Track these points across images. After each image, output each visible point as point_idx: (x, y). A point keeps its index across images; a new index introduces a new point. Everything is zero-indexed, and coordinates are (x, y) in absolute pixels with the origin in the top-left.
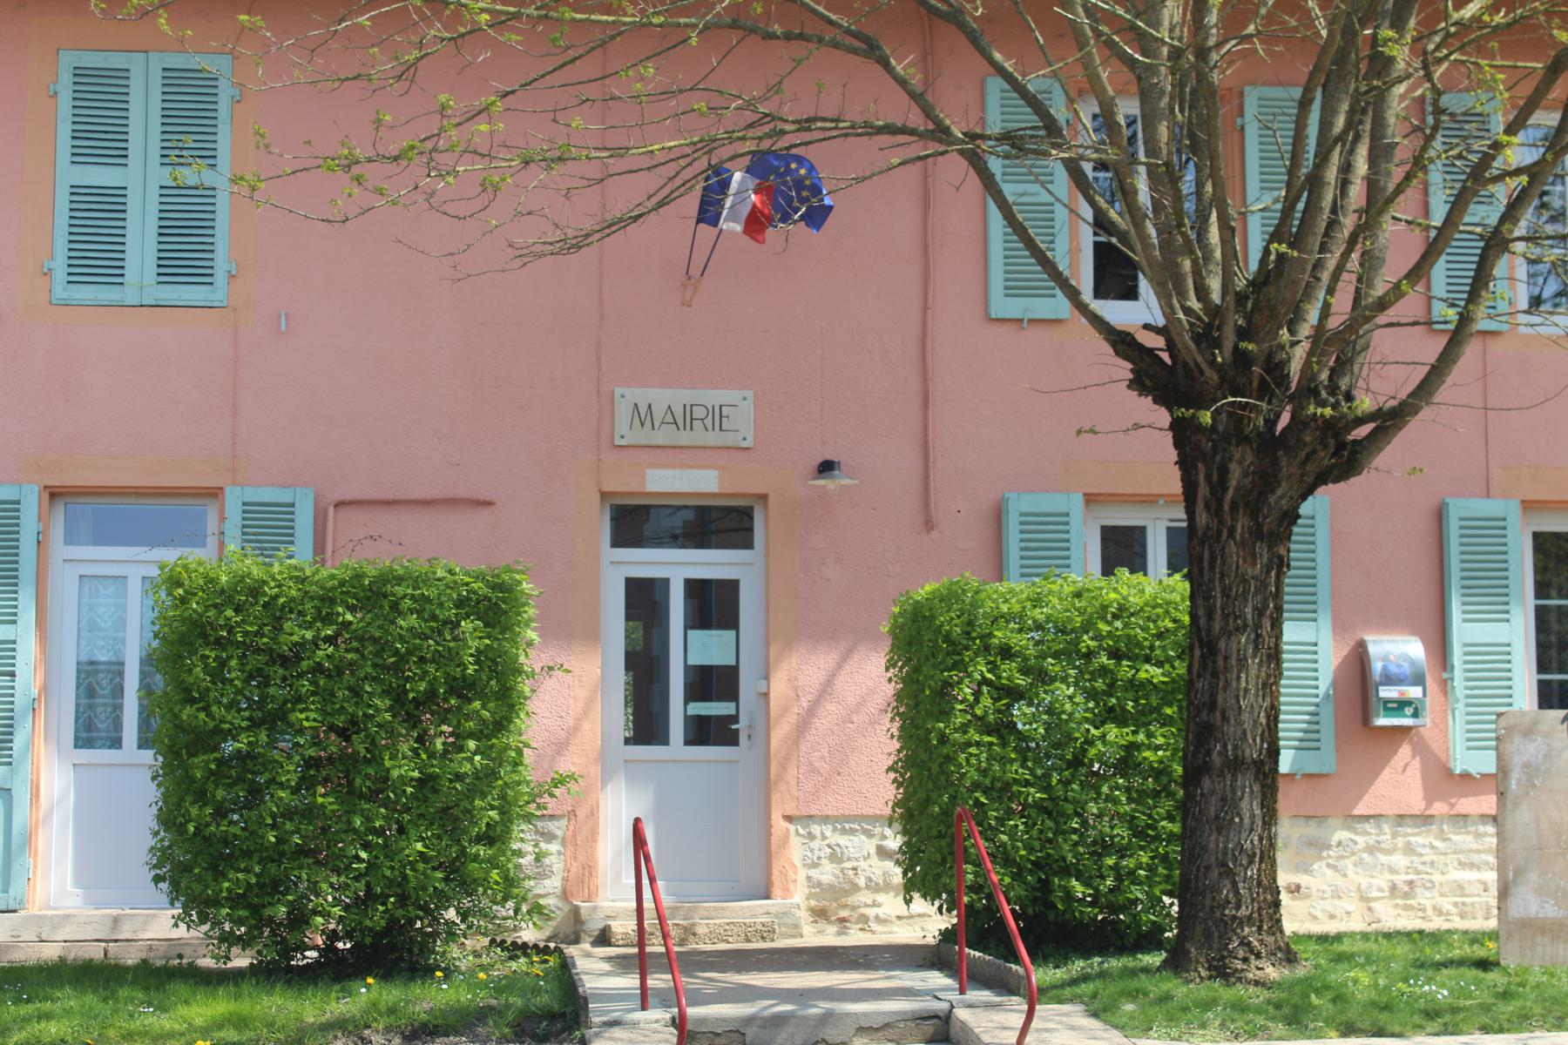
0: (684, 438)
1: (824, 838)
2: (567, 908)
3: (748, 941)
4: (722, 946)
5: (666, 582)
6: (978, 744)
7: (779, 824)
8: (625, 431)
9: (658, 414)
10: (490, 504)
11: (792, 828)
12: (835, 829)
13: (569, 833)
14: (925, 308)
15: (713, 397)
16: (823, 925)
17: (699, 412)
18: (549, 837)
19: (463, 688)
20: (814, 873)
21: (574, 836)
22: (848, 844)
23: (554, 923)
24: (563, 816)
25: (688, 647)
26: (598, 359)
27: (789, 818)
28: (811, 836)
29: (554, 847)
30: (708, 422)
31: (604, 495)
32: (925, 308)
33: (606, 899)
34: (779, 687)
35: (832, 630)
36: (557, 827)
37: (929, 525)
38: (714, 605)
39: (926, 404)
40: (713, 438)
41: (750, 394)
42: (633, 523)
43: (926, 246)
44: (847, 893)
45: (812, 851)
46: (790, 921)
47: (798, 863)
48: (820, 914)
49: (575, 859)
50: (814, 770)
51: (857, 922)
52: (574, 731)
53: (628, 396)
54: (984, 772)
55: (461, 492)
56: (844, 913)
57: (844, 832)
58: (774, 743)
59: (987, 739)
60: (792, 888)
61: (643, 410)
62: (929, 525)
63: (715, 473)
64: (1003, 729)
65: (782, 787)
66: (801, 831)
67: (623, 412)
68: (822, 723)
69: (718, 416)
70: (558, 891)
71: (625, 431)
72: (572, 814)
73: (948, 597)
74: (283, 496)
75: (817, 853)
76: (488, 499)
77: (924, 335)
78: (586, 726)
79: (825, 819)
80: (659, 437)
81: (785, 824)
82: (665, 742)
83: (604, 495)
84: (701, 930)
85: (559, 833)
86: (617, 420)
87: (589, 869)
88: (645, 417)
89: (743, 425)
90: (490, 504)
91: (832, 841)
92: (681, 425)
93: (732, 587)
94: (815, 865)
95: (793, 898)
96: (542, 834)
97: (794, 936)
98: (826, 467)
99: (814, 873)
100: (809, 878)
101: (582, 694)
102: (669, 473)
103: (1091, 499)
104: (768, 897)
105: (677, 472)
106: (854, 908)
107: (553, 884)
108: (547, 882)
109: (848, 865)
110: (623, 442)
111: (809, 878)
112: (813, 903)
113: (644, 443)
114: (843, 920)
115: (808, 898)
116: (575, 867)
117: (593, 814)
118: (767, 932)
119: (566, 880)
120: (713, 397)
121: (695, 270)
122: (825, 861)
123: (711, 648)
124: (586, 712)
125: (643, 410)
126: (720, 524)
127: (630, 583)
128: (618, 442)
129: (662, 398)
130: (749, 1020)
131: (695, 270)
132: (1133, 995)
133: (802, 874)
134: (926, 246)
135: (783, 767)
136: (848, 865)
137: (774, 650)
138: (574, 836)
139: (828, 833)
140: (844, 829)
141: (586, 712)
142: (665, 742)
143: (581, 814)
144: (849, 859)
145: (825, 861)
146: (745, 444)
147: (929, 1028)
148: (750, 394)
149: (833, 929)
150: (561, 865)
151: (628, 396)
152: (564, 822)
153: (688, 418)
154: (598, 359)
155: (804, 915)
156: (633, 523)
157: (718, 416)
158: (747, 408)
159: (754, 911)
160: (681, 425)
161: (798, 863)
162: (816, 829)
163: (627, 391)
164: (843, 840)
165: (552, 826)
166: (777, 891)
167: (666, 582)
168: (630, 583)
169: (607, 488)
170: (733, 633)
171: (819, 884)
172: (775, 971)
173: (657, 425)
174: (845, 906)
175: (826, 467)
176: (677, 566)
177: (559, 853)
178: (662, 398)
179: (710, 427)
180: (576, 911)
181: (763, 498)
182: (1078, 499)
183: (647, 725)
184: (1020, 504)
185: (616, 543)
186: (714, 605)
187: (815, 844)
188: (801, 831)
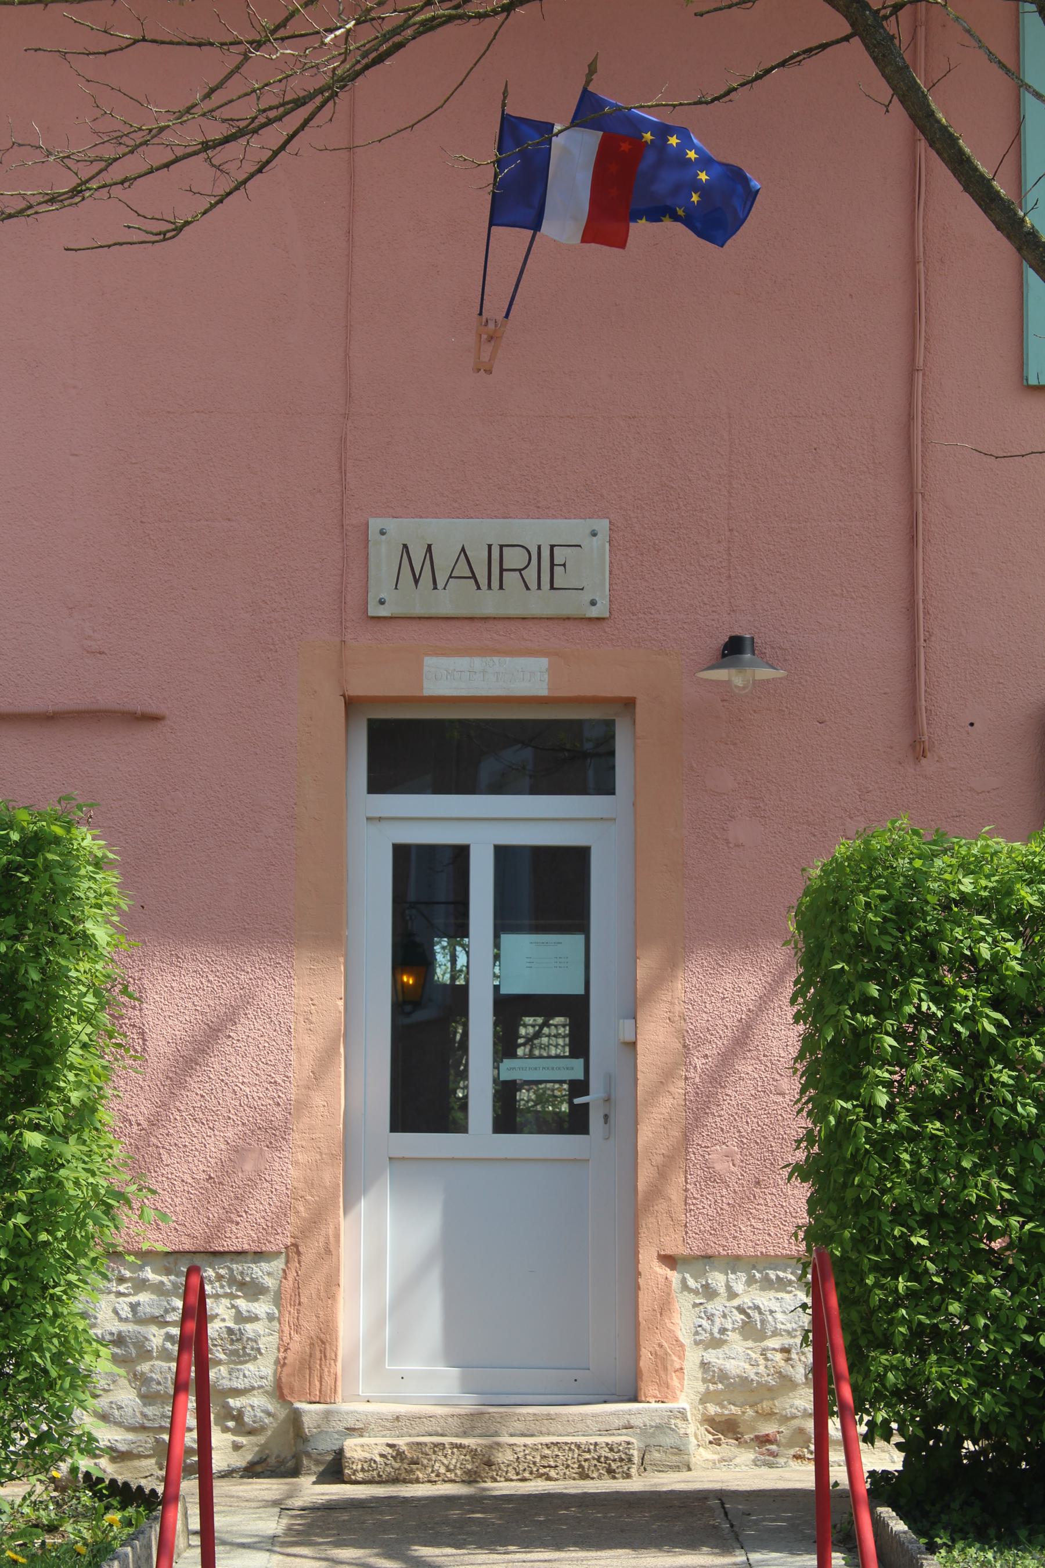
0: (490, 603)
1: (732, 1295)
2: (282, 1414)
3: (584, 1476)
4: (537, 1486)
5: (461, 853)
6: (913, 1137)
7: (653, 1272)
8: (387, 593)
9: (444, 562)
10: (156, 719)
11: (675, 1277)
12: (751, 1281)
13: (289, 1284)
14: (912, 370)
15: (534, 531)
16: (728, 1447)
17: (514, 558)
18: (253, 1290)
20: (713, 1356)
21: (297, 1290)
22: (774, 1306)
23: (261, 1439)
24: (278, 1254)
25: (485, 962)
26: (342, 471)
27: (670, 1261)
28: (710, 1293)
29: (262, 1307)
30: (531, 574)
31: (352, 704)
32: (912, 370)
33: (356, 1398)
34: (655, 1037)
35: (700, 927)
38: (549, 890)
39: (913, 539)
40: (541, 603)
41: (602, 525)
42: (413, 750)
43: (913, 263)
44: (771, 1392)
45: (710, 1318)
46: (668, 1440)
47: (686, 1339)
48: (725, 1428)
49: (297, 1328)
50: (713, 1178)
51: (790, 1445)
52: (302, 1105)
53: (391, 532)
54: (926, 1186)
55: (107, 699)
56: (769, 1429)
57: (767, 1284)
59: (934, 1127)
60: (675, 1382)
61: (418, 555)
62: (918, 749)
63: (544, 662)
64: (967, 1107)
65: (661, 1206)
66: (691, 1283)
70: (268, 1383)
71: (387, 593)
72: (294, 1250)
75: (718, 1321)
76: (153, 708)
77: (910, 417)
78: (318, 1100)
79: (734, 1263)
81: (662, 1271)
82: (460, 1127)
83: (352, 704)
84: (504, 1457)
85: (269, 1282)
86: (372, 572)
87: (322, 1345)
88: (417, 566)
89: (591, 577)
90: (156, 719)
91: (746, 1300)
92: (483, 581)
93: (580, 856)
94: (716, 1343)
95: (682, 1400)
96: (242, 1285)
97: (677, 1468)
98: (972, 724)
99: (713, 1356)
100: (704, 1365)
101: (311, 1044)
102: (462, 663)
104: (635, 1399)
105: (478, 662)
106: (785, 1419)
107: (261, 1370)
108: (250, 1368)
109: (774, 1343)
110: (383, 611)
111: (704, 1365)
112: (712, 1409)
113: (419, 611)
114: (764, 1440)
115: (703, 1401)
116: (298, 1343)
117: (329, 1251)
118: (616, 1463)
119: (280, 1363)
120: (534, 531)
121: (495, 307)
122: (733, 1336)
123: (536, 962)
125: (418, 555)
126: (565, 751)
127: (402, 853)
128: (374, 610)
129: (449, 534)
131: (495, 307)
133: (692, 1358)
134: (913, 263)
135: (663, 1174)
136: (774, 1343)
137: (644, 968)
138: (297, 1290)
139: (739, 1287)
140: (766, 1279)
142: (460, 1127)
143: (309, 1253)
144: (776, 1333)
145: (733, 1336)
146: (594, 612)
148: (602, 525)
149: (746, 1456)
150: (274, 1339)
151: (391, 532)
152: (279, 1264)
153: (497, 569)
154: (342, 471)
155: (694, 1431)
156: (413, 750)
157: (548, 564)
158: (598, 548)
159: (595, 1422)
160: (483, 581)
161: (686, 1339)
162: (718, 1279)
163: (390, 524)
164: (766, 1300)
165: (259, 1271)
166: (649, 1389)
167: (461, 853)
168: (402, 853)
169: (357, 690)
170: (580, 938)
171: (723, 1376)
172: (544, 1545)
173: (440, 584)
174: (770, 1415)
175: (972, 724)
176: (484, 823)
177: (270, 1317)
178: (449, 534)
179: (533, 585)
180: (295, 1418)
181: (629, 704)
183: (423, 1095)
185: (377, 785)
187: (716, 1306)
188: (691, 1283)
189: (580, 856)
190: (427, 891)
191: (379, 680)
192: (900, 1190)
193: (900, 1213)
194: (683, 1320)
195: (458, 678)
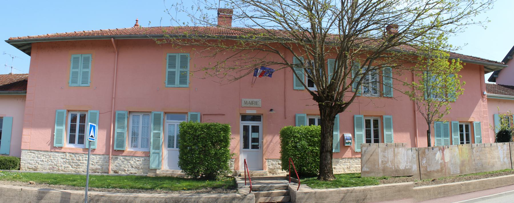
0: (252, 106)
7: (264, 160)
15: (255, 100)
18: (232, 161)
19: (221, 141)
25: (252, 135)
34: (264, 141)
35: (272, 133)
36: (234, 160)
37: (285, 118)
38: (255, 129)
40: (256, 106)
42: (244, 118)
48: (270, 172)
52: (236, 147)
53: (244, 100)
58: (264, 148)
62: (285, 118)
64: (296, 147)
67: (243, 102)
68: (270, 146)
69: (256, 103)
71: (243, 105)
73: (288, 129)
74: (196, 113)
79: (271, 159)
80: (248, 106)
87: (238, 166)
88: (246, 103)
89: (260, 104)
93: (258, 126)
98: (271, 110)
101: (237, 142)
103: (307, 115)
107: (233, 168)
118: (263, 175)
120: (255, 100)
123: (255, 135)
124: (238, 144)
126: (256, 118)
129: (248, 100)
130: (260, 187)
132: (313, 183)
141: (238, 144)
147: (285, 188)
151: (244, 100)
153: (252, 103)
156: (244, 118)
157: (256, 103)
175: (271, 110)
176: (250, 124)
178: (248, 100)
181: (262, 114)
182: (306, 115)
183: (246, 146)
184: (298, 115)
186: (255, 129)
189: (258, 126)
190: (246, 128)
191: (243, 112)
192: (291, 153)
193: (291, 155)
194: (267, 164)
195: (249, 112)
